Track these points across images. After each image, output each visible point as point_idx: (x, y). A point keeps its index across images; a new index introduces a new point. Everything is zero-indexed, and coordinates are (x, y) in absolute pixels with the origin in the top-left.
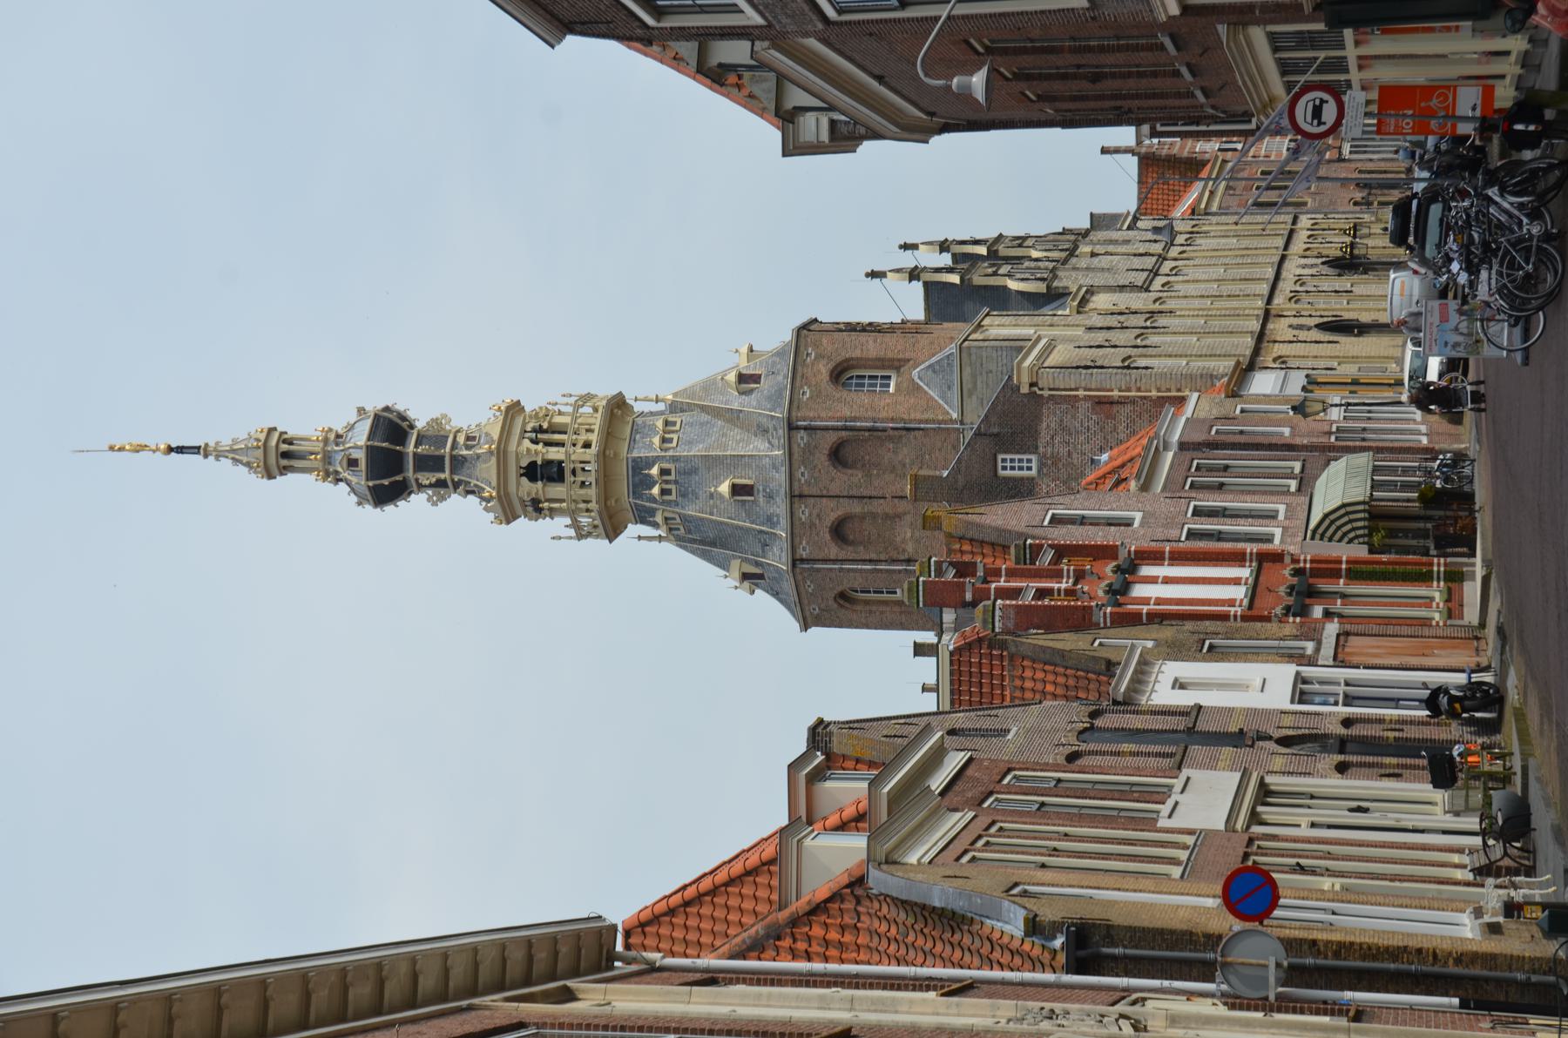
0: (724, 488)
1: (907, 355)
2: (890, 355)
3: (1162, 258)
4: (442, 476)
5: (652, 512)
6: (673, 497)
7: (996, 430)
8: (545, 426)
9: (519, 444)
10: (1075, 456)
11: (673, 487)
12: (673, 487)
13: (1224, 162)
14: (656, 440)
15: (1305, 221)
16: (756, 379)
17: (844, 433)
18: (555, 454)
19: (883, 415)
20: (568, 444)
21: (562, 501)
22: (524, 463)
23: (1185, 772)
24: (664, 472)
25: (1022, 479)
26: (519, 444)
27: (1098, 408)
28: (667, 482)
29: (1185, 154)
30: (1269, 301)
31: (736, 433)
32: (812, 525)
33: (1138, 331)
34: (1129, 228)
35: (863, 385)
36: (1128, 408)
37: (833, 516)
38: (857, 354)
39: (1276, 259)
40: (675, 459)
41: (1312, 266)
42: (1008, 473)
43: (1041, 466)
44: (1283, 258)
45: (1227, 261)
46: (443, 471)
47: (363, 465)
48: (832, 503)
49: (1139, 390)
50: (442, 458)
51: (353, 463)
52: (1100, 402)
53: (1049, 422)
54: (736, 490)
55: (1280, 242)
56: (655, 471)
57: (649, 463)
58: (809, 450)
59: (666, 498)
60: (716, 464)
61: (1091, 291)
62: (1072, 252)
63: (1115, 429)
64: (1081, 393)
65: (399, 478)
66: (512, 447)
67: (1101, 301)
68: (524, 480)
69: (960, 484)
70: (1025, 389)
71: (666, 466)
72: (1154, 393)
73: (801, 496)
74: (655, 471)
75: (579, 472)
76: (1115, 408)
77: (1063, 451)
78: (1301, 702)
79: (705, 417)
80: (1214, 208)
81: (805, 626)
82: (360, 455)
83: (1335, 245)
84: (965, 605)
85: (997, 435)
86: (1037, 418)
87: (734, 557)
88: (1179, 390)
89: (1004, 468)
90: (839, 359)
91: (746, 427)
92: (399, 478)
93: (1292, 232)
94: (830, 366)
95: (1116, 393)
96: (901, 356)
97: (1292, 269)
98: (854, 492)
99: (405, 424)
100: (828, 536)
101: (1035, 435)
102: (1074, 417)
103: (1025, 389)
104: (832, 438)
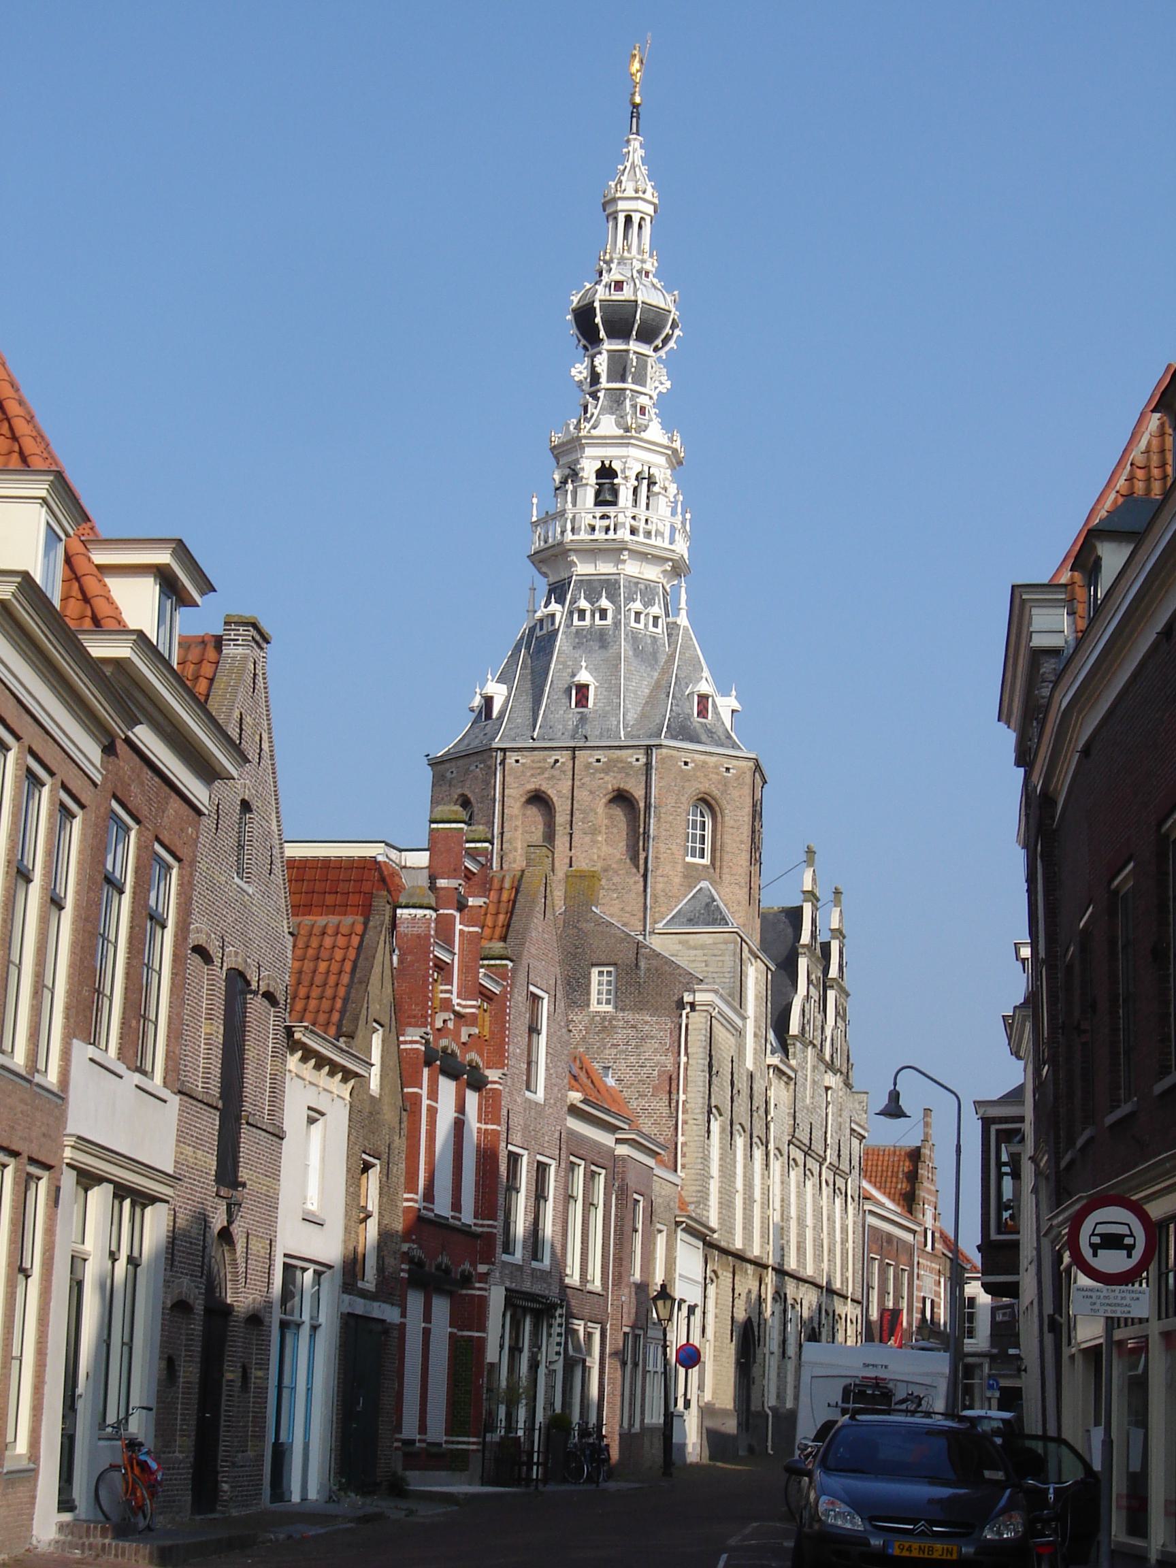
0: (584, 677)
1: (726, 877)
2: (726, 857)
3: (822, 1161)
4: (603, 379)
5: (561, 600)
6: (576, 622)
7: (642, 964)
8: (656, 489)
9: (637, 460)
10: (614, 1051)
11: (587, 622)
12: (587, 622)
13: (914, 1232)
16: (702, 713)
17: (642, 805)
18: (625, 495)
19: (662, 847)
20: (635, 511)
21: (574, 504)
22: (616, 466)
23: (175, 1100)
24: (603, 614)
25: (589, 993)
26: (637, 460)
27: (666, 1077)
28: (593, 616)
29: (923, 1194)
32: (543, 770)
33: (748, 1127)
34: (852, 1130)
35: (694, 828)
36: (665, 1111)
37: (551, 792)
40: (617, 624)
43: (604, 1017)
46: (608, 382)
47: (617, 296)
48: (566, 790)
49: (685, 1122)
50: (623, 380)
51: (619, 286)
53: (655, 1025)
54: (582, 689)
56: (604, 603)
57: (612, 598)
59: (576, 616)
62: (830, 1067)
63: (642, 1096)
64: (683, 1059)
65: (602, 334)
67: (779, 1093)
68: (599, 465)
69: (584, 925)
71: (610, 614)
72: (681, 1139)
73: (574, 758)
74: (604, 603)
75: (606, 522)
77: (620, 1036)
78: (286, 1267)
80: (871, 1220)
81: (435, 763)
82: (627, 294)
84: (432, 879)
86: (655, 1011)
87: (510, 690)
88: (683, 1167)
89: (601, 973)
90: (724, 803)
92: (602, 334)
94: (716, 793)
95: (682, 1097)
96: (725, 870)
98: (577, 815)
99: (658, 342)
100: (531, 787)
101: (639, 1007)
104: (639, 793)
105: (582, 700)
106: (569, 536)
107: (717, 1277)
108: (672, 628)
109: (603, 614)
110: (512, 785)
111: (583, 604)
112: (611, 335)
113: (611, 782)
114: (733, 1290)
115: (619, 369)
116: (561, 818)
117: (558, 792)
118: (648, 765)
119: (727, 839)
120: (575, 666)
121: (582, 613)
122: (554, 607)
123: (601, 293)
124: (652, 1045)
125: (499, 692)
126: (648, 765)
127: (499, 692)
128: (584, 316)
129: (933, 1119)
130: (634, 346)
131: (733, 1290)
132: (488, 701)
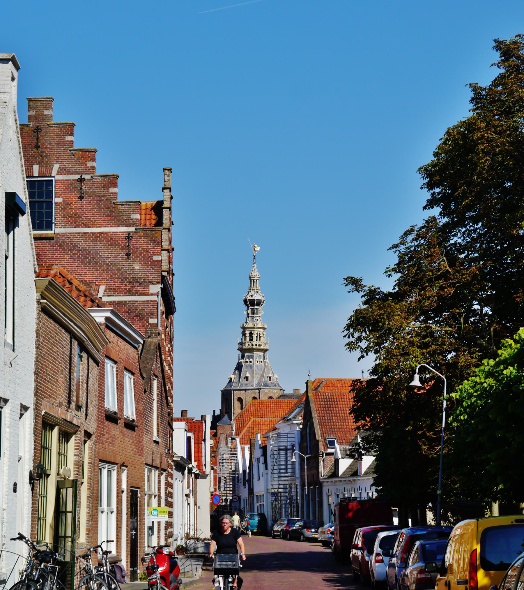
0: (248, 375)
5: (243, 359)
14: (257, 360)
16: (270, 380)
18: (255, 338)
22: (253, 332)
24: (251, 362)
31: (259, 377)
40: (253, 364)
47: (252, 298)
51: (252, 296)
56: (251, 360)
57: (253, 358)
58: (255, 393)
60: (253, 372)
66: (255, 329)
74: (251, 360)
79: (263, 369)
82: (253, 298)
91: (260, 379)
105: (247, 380)
106: (244, 347)
108: (265, 363)
109: (251, 362)
110: (236, 395)
111: (247, 360)
112: (251, 306)
115: (253, 313)
116: (244, 402)
117: (243, 398)
118: (259, 392)
120: (246, 372)
121: (247, 362)
122: (242, 360)
123: (249, 298)
125: (233, 376)
126: (259, 392)
127: (233, 376)
128: (245, 301)
130: (256, 307)
132: (231, 379)
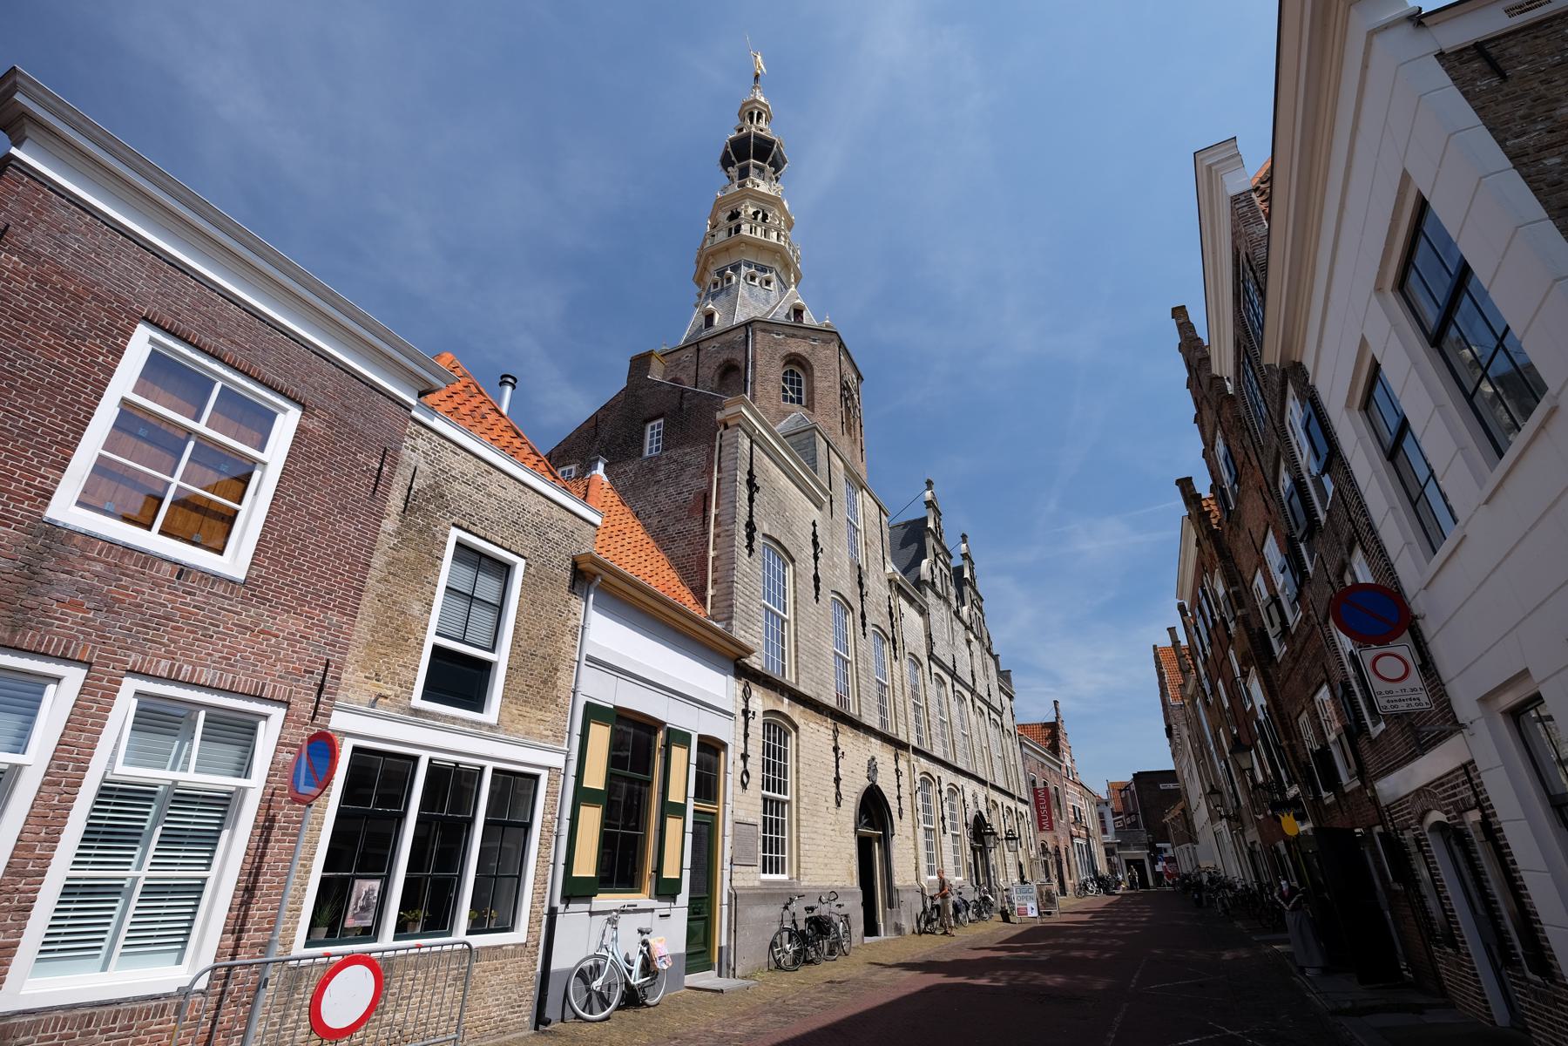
15: (1023, 808)
19: (758, 388)
27: (701, 497)
30: (916, 751)
33: (857, 606)
38: (817, 374)
39: (982, 776)
41: (976, 803)
42: (648, 432)
44: (983, 782)
45: (975, 737)
49: (717, 536)
51: (740, 130)
52: (706, 497)
55: (1001, 784)
61: (923, 612)
67: (910, 615)
69: (640, 392)
70: (719, 416)
76: (699, 516)
77: (661, 475)
83: (997, 823)
85: (681, 409)
93: (1012, 796)
97: (970, 787)
102: (694, 475)
103: (719, 416)
104: (740, 357)
107: (796, 728)
113: (725, 356)
114: (836, 749)
119: (816, 384)
124: (691, 470)
129: (1060, 706)
131: (836, 749)
